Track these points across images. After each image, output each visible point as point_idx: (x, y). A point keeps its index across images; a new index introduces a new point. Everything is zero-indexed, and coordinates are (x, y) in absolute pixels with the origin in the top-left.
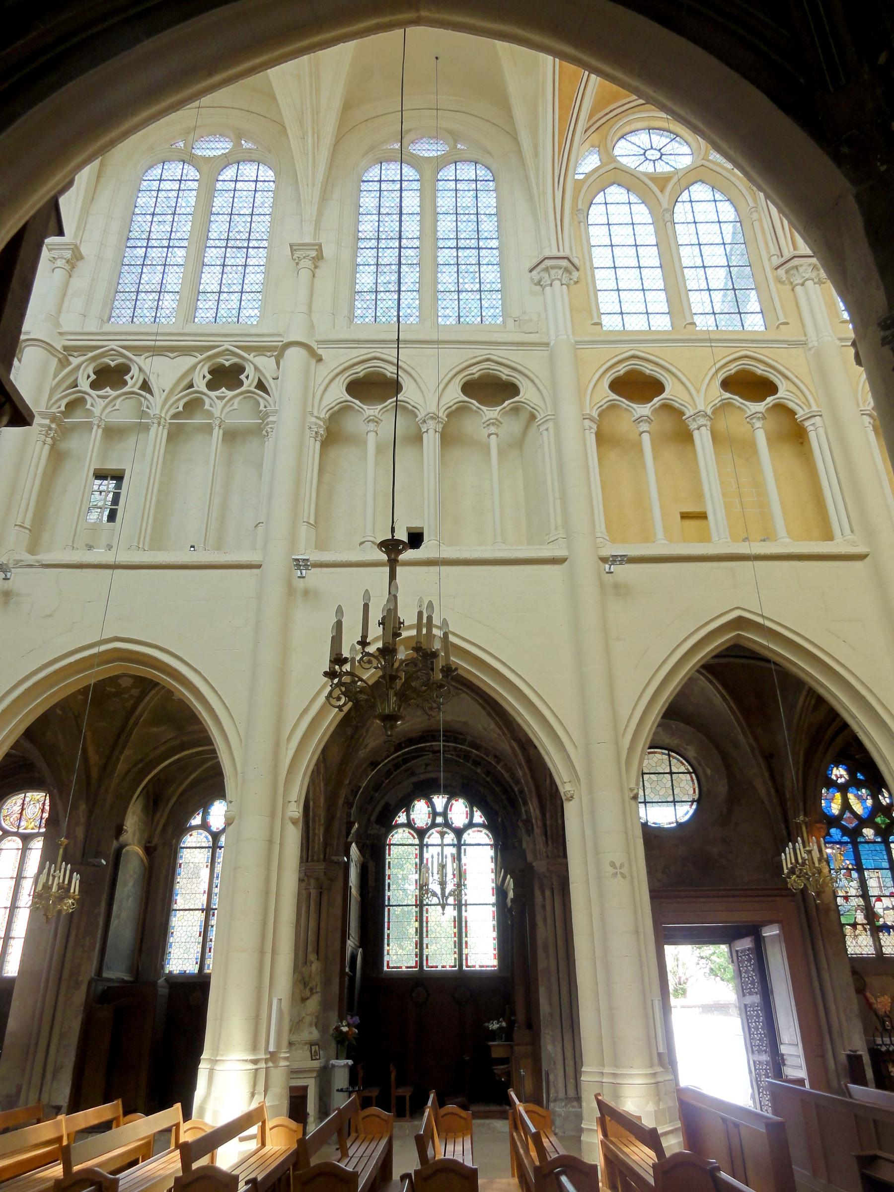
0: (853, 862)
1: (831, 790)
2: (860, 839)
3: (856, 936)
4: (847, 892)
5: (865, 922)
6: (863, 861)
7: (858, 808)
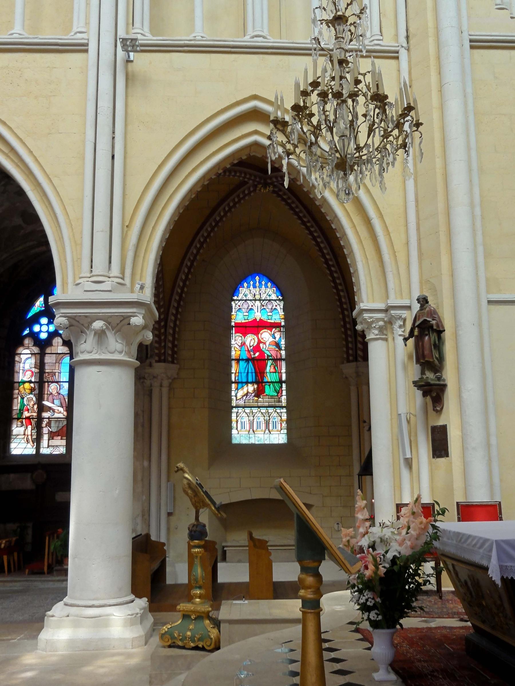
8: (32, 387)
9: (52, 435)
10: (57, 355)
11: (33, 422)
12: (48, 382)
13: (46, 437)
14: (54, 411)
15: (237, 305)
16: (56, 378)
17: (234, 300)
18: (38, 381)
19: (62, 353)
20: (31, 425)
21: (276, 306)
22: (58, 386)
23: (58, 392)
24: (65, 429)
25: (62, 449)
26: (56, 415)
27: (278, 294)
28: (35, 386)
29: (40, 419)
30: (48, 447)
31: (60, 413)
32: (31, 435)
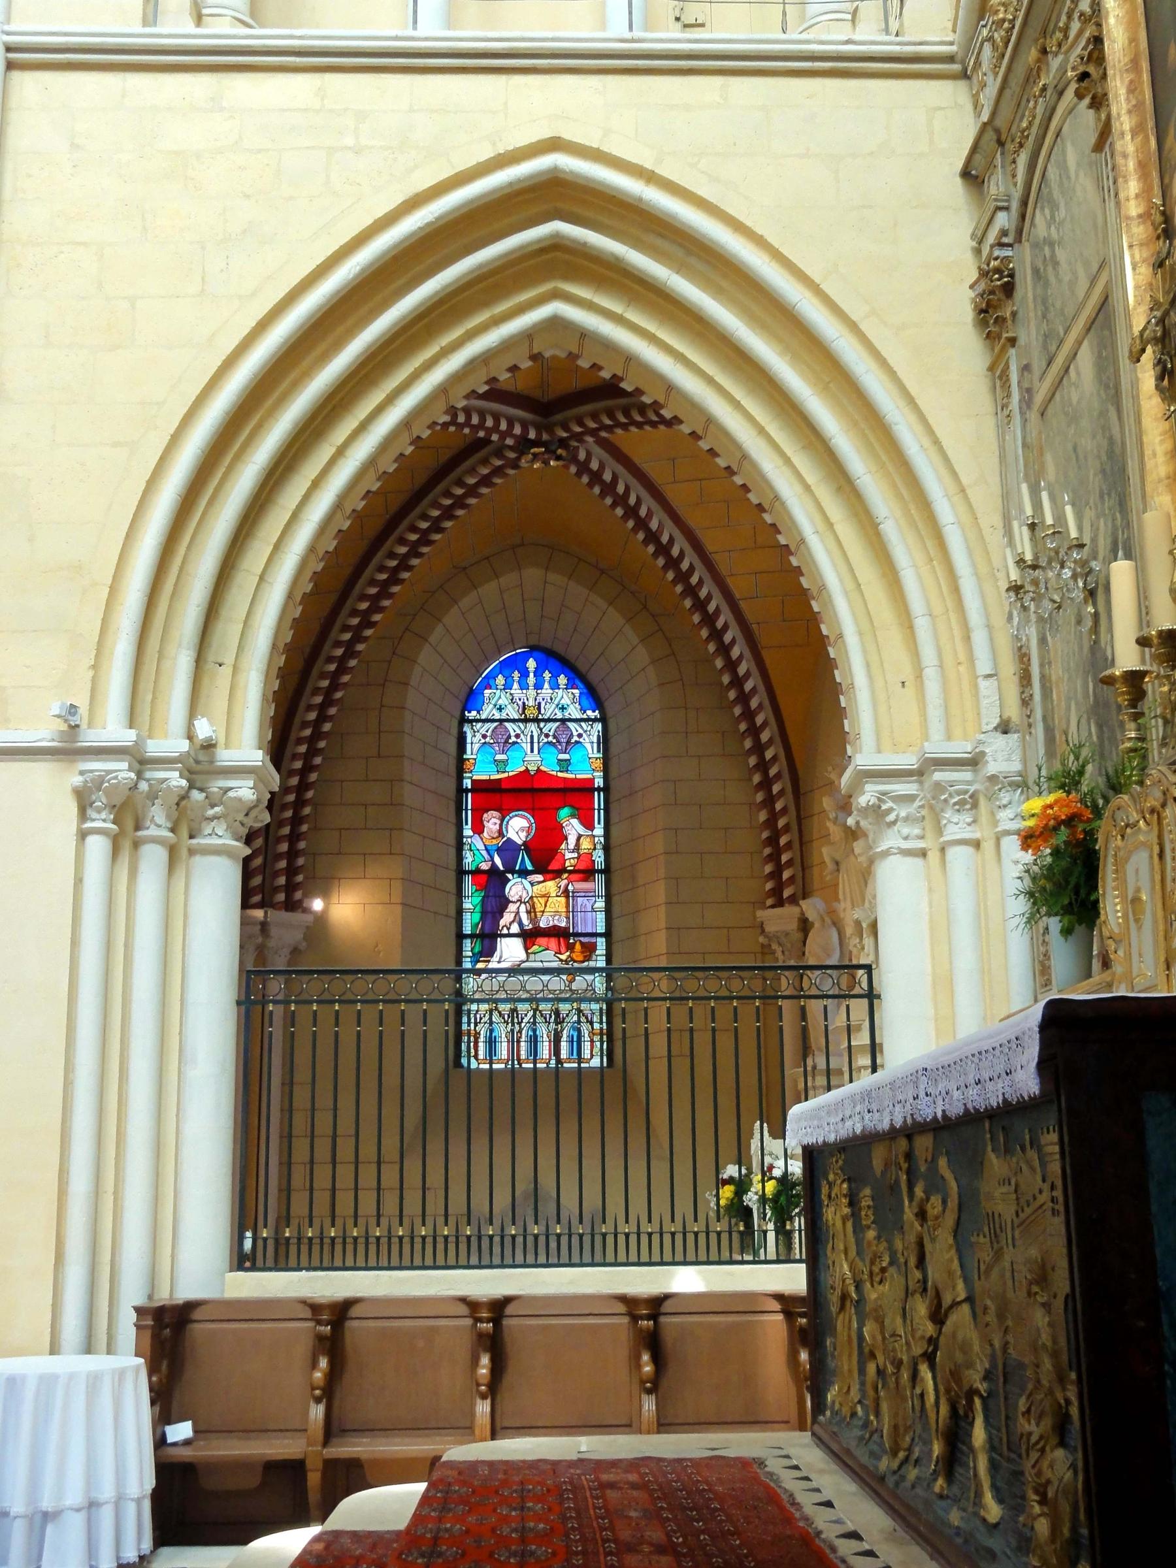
15: (479, 736)
17: (471, 721)
21: (580, 736)
27: (585, 703)
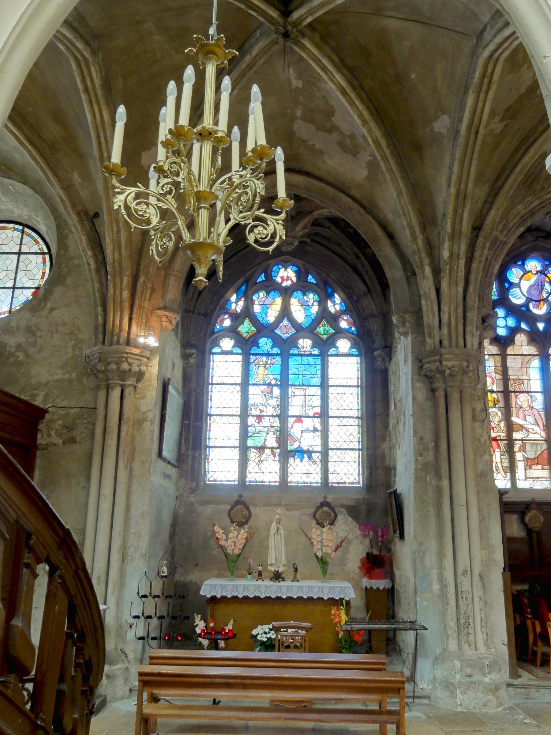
0: (279, 377)
1: (272, 294)
2: (294, 351)
3: (261, 461)
4: (262, 411)
5: (276, 445)
6: (291, 377)
7: (299, 314)
8: (494, 398)
9: (529, 463)
10: (523, 357)
11: (502, 444)
12: (515, 392)
13: (520, 466)
14: (527, 431)
16: (524, 388)
18: (501, 389)
19: (529, 355)
20: (499, 447)
22: (529, 397)
23: (529, 406)
24: (545, 455)
25: (545, 482)
26: (532, 436)
28: (498, 397)
29: (510, 442)
30: (526, 480)
31: (536, 433)
32: (501, 462)
